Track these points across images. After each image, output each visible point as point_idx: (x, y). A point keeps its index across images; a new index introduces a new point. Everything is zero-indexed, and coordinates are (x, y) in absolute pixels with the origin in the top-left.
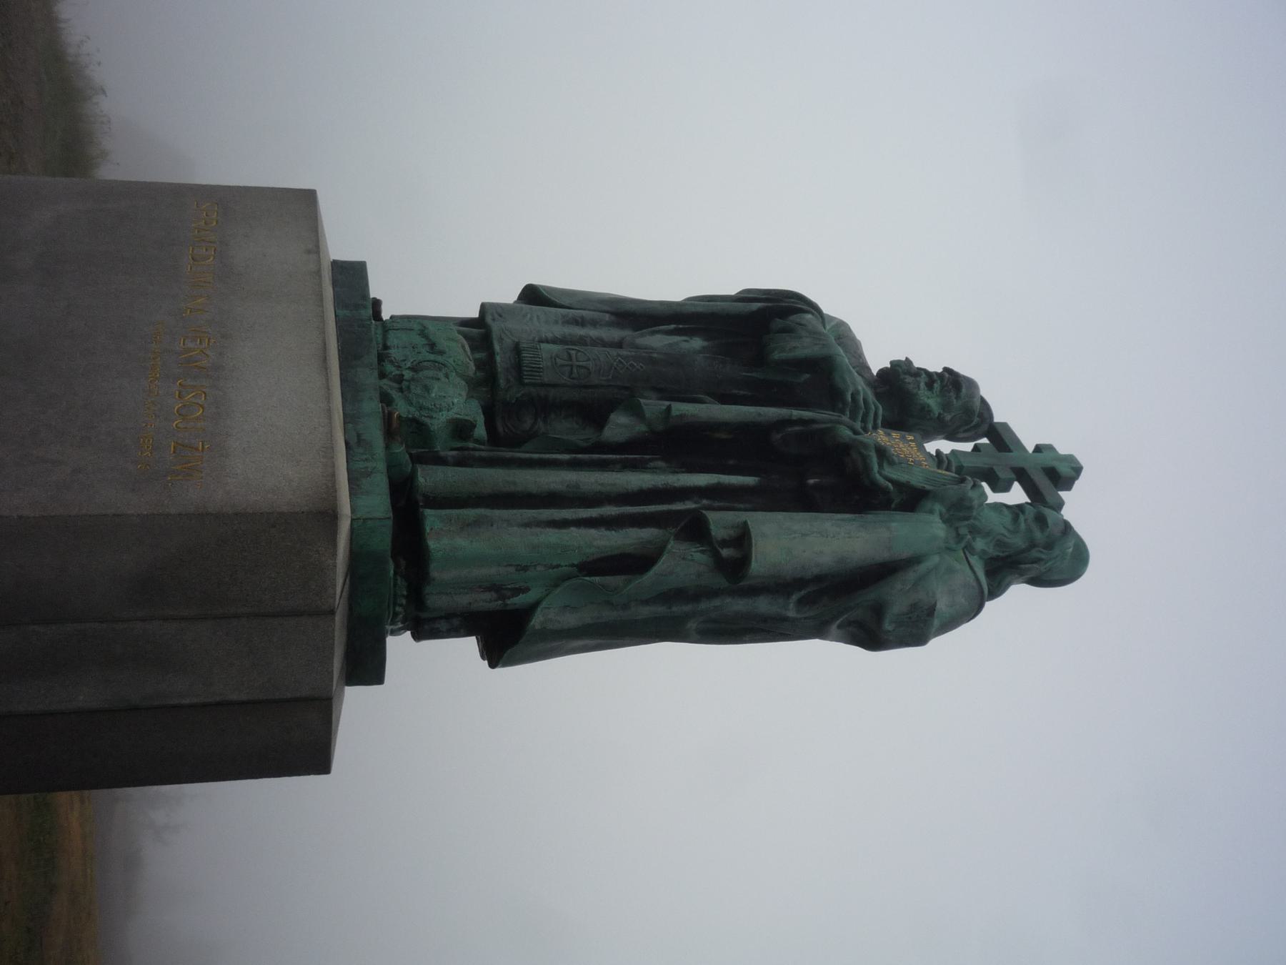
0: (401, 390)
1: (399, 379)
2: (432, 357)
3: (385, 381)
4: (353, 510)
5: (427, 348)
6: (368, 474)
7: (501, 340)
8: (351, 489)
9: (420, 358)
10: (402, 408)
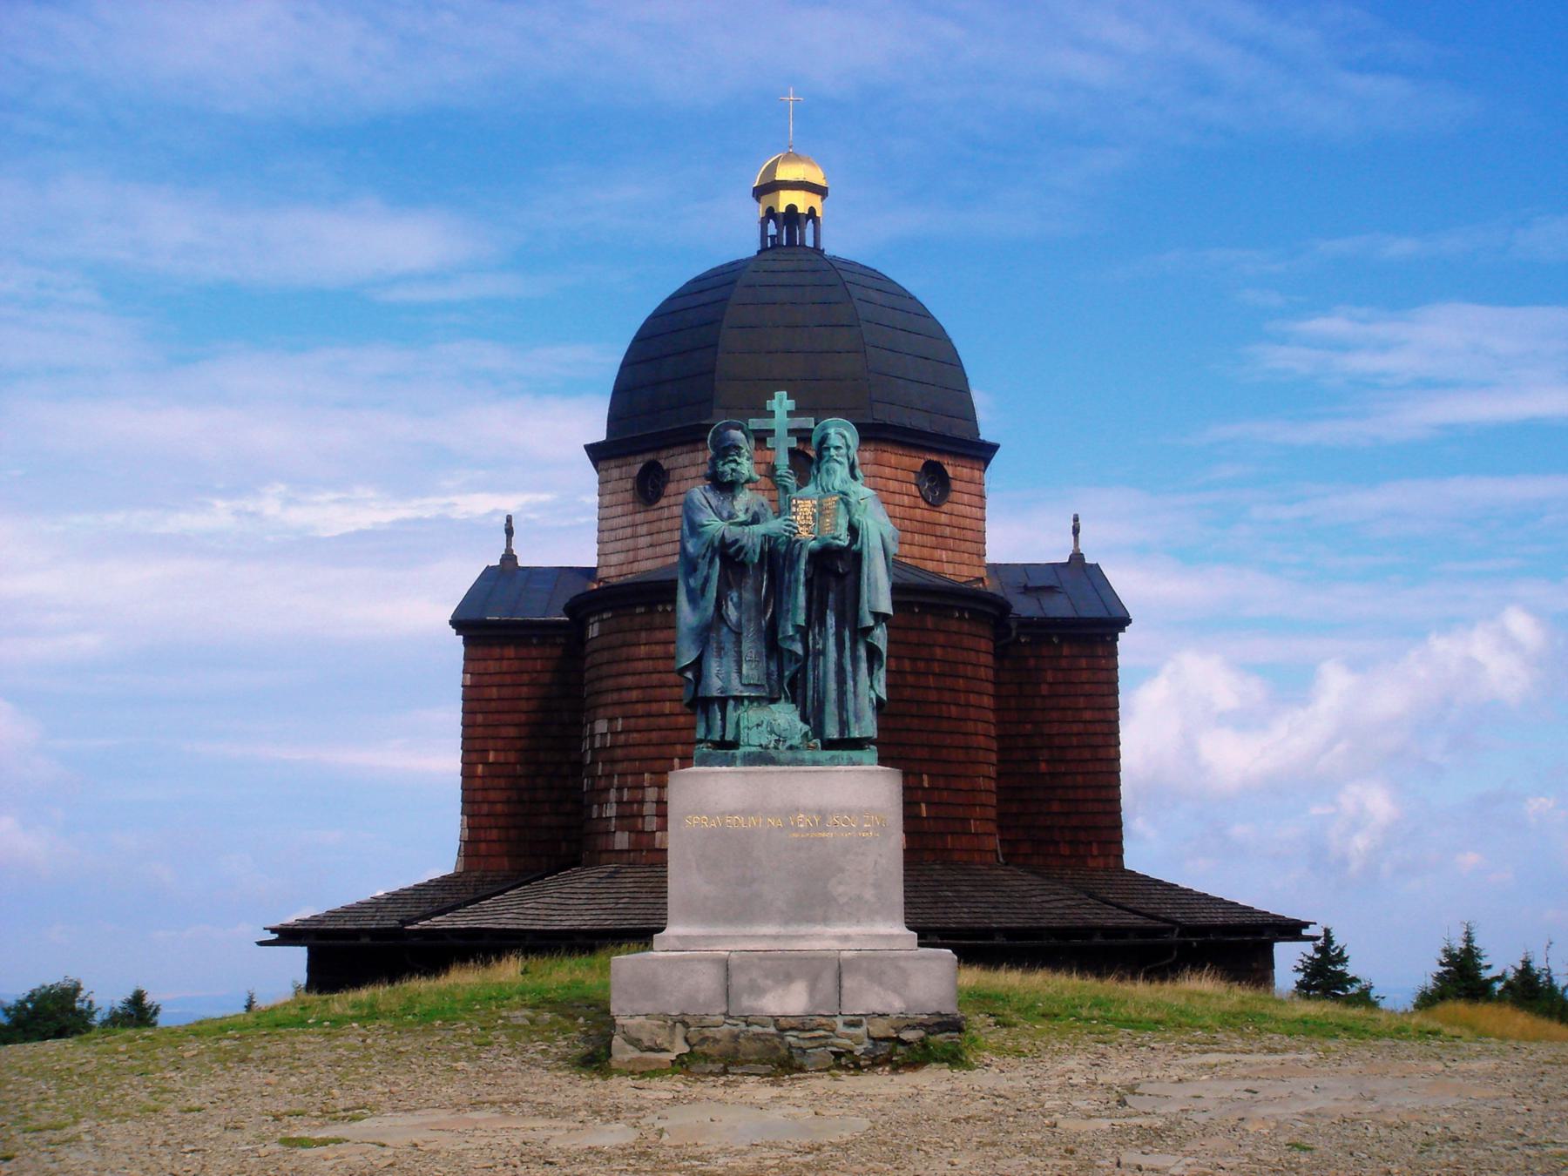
0: (785, 741)
1: (777, 741)
2: (764, 726)
3: (780, 747)
4: (872, 765)
5: (760, 728)
6: (851, 759)
7: (741, 692)
8: (859, 765)
9: (765, 732)
10: (796, 741)
